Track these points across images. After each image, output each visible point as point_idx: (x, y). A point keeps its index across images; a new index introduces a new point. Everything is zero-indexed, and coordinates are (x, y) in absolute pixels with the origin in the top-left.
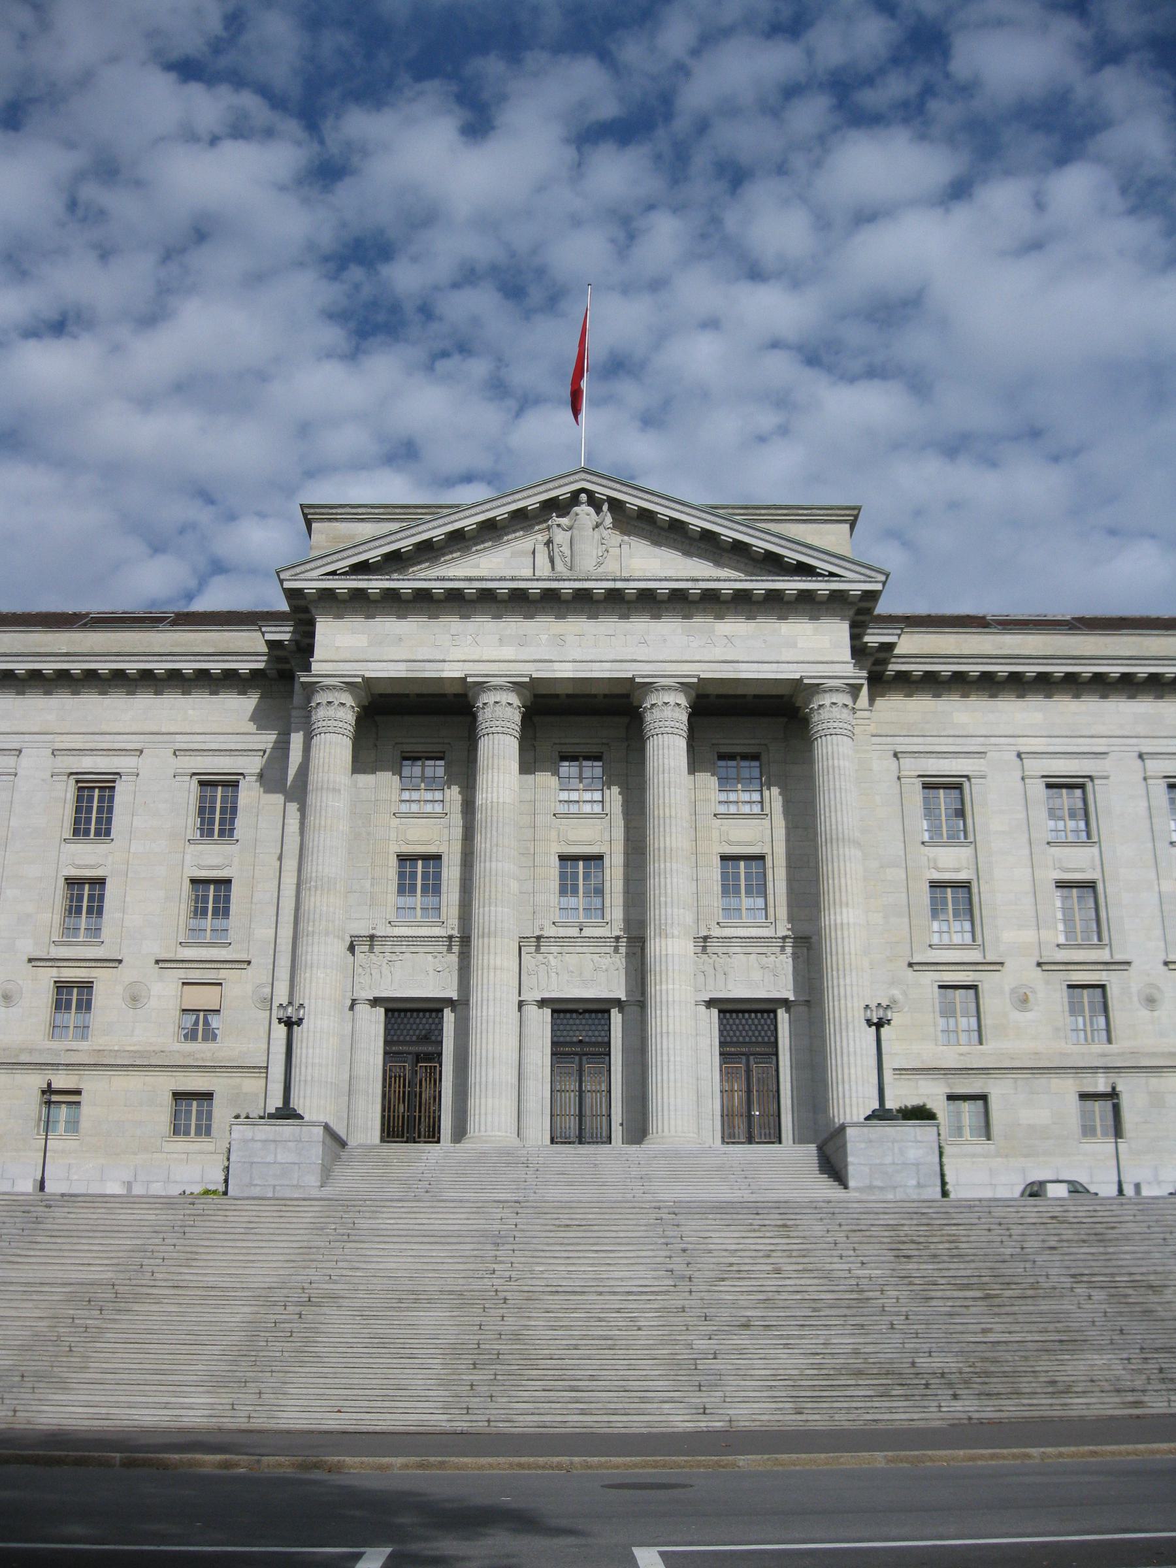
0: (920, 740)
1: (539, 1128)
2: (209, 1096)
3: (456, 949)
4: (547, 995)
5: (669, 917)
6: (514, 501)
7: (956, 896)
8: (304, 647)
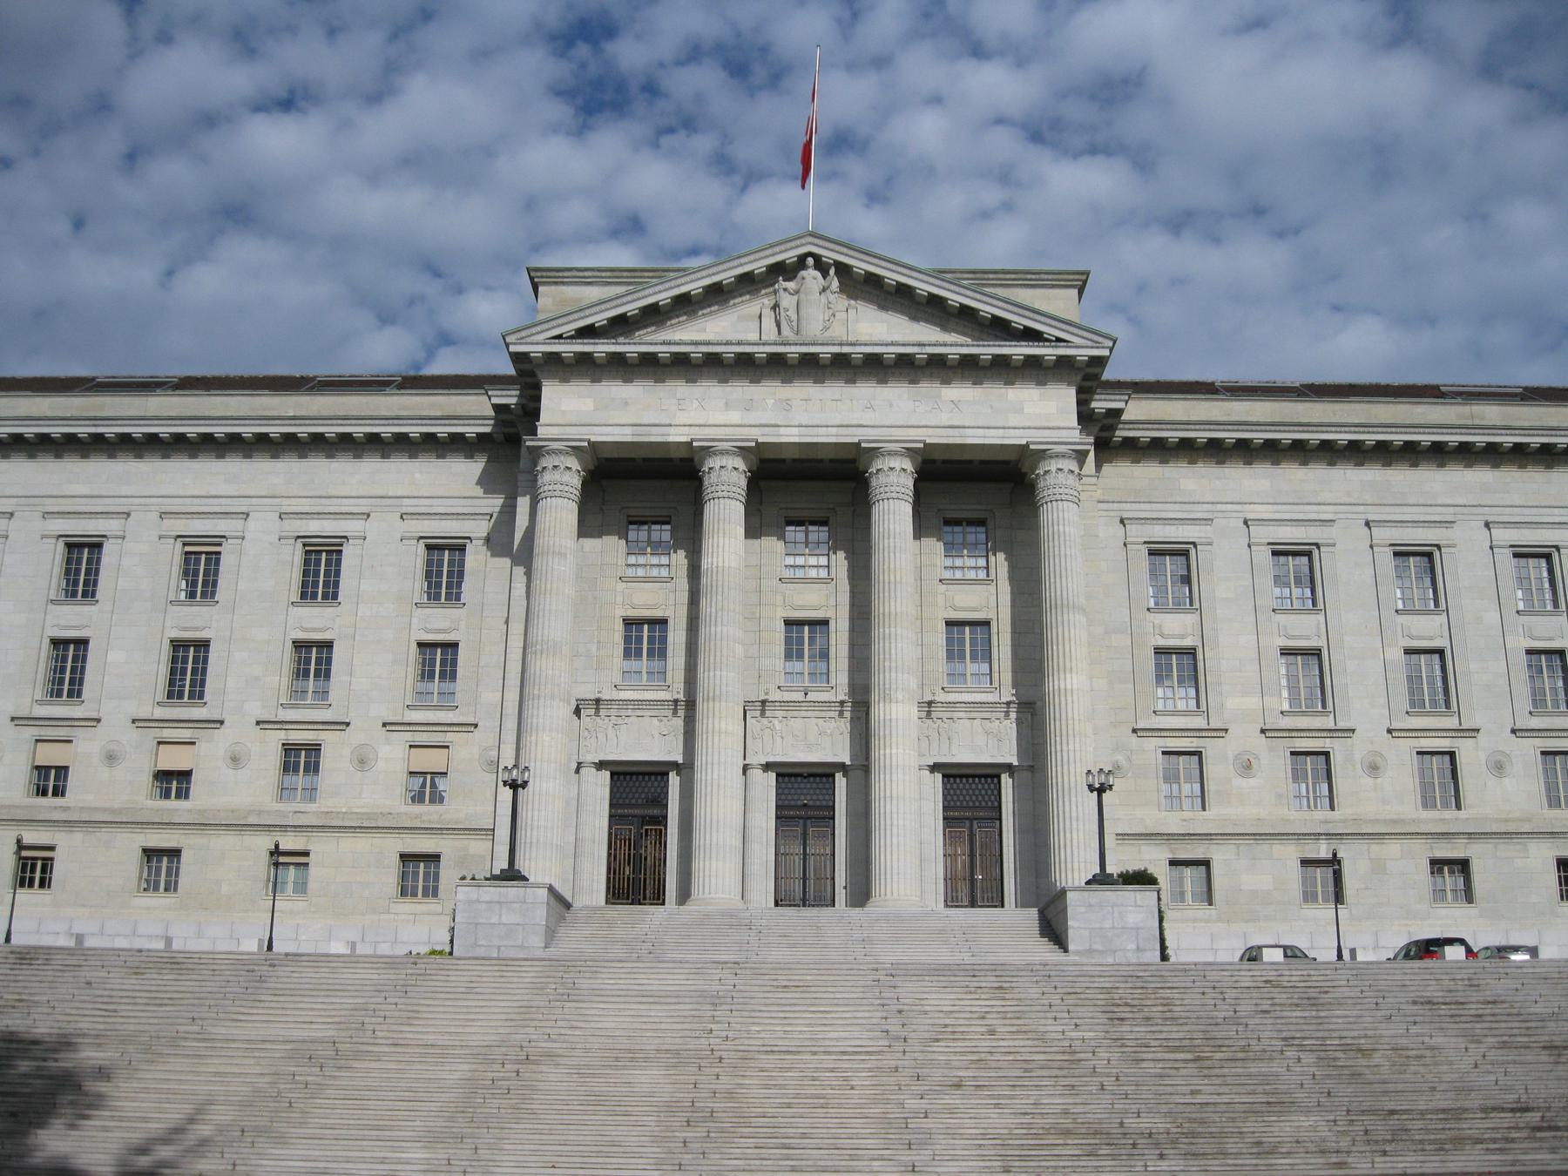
0: (1147, 506)
1: (763, 889)
2: (434, 858)
3: (681, 713)
4: (771, 759)
7: (1181, 663)
8: (530, 411)
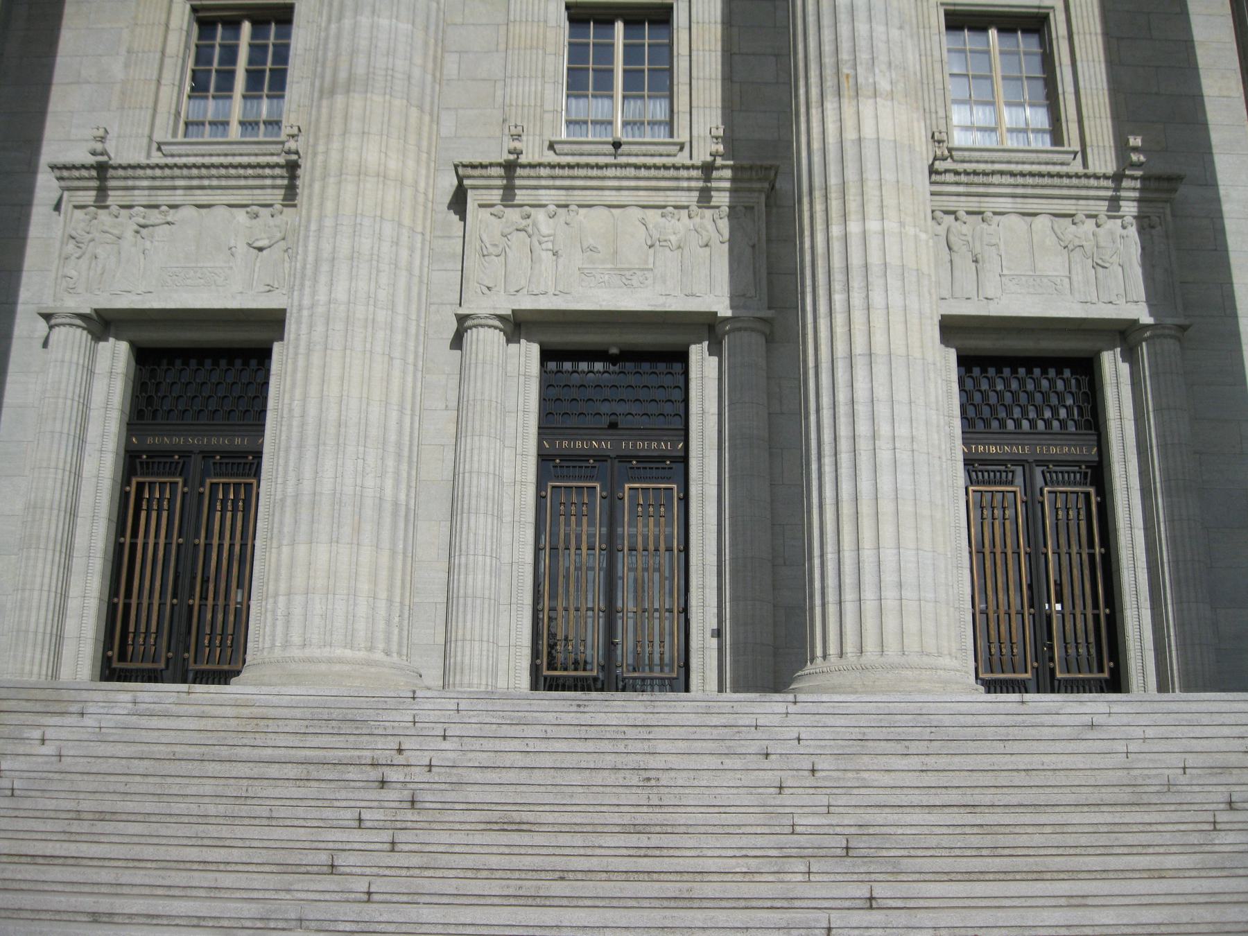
1: (501, 642)
4: (527, 304)
5: (863, 43)
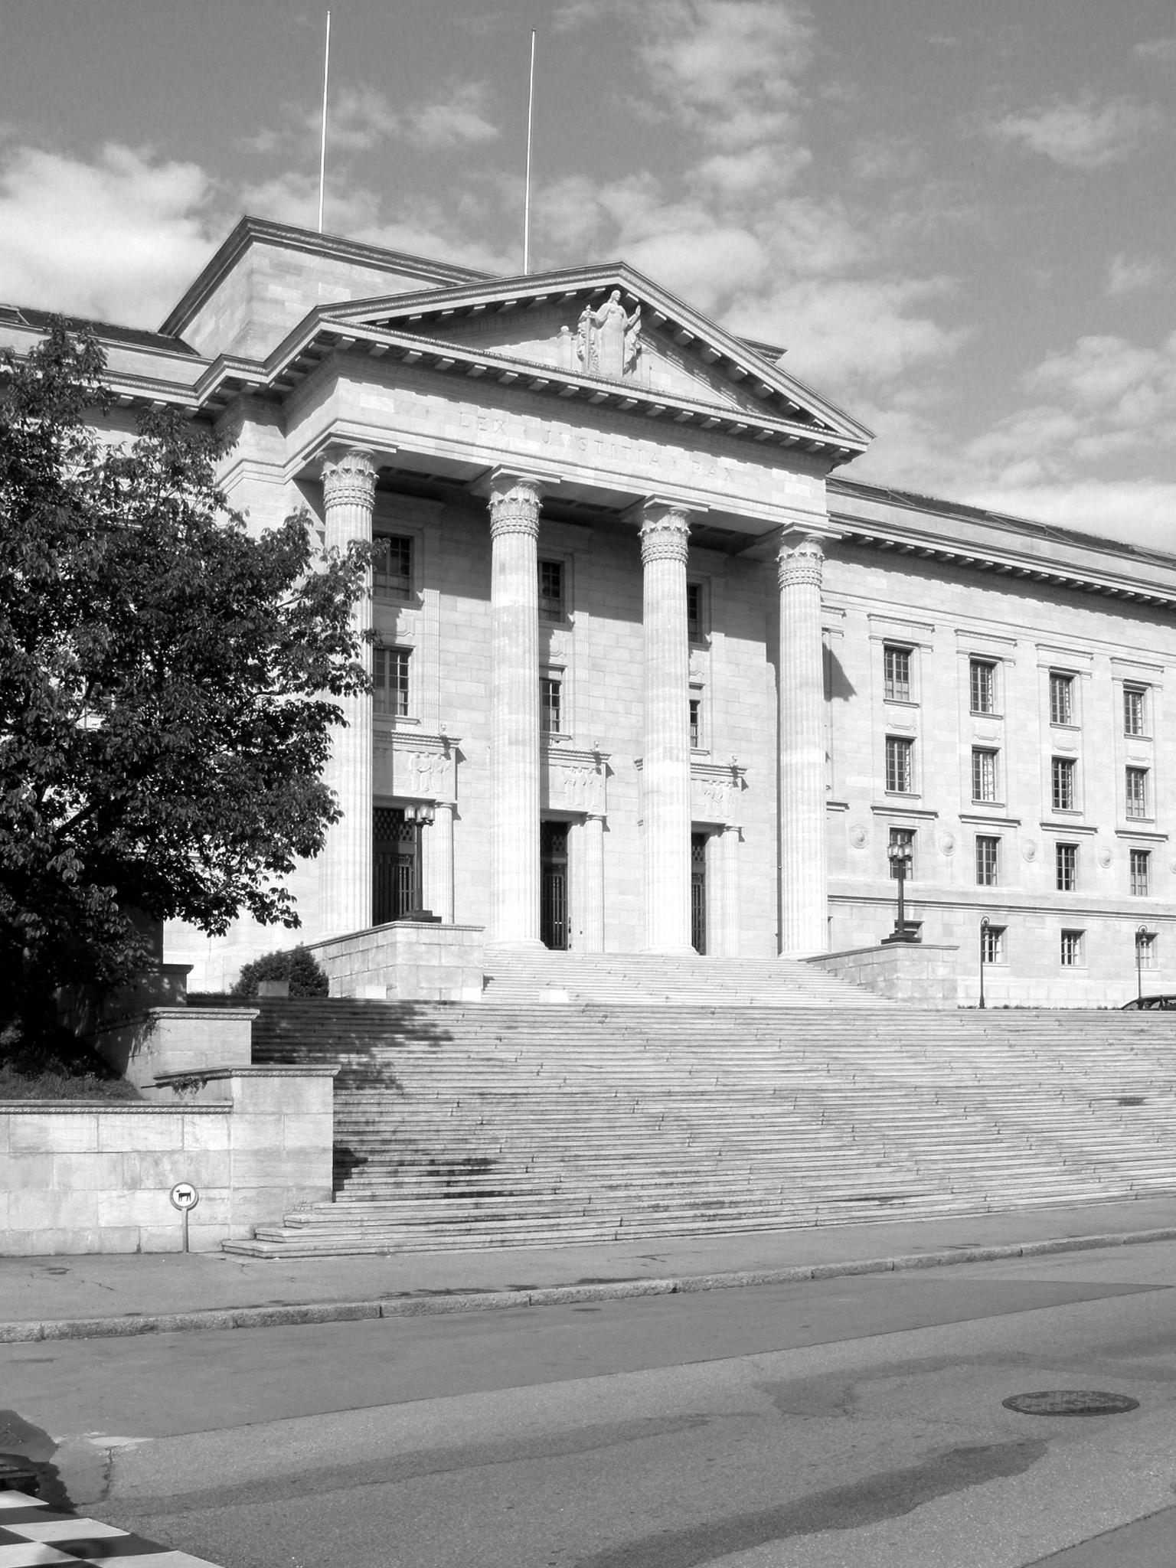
6: (555, 284)
